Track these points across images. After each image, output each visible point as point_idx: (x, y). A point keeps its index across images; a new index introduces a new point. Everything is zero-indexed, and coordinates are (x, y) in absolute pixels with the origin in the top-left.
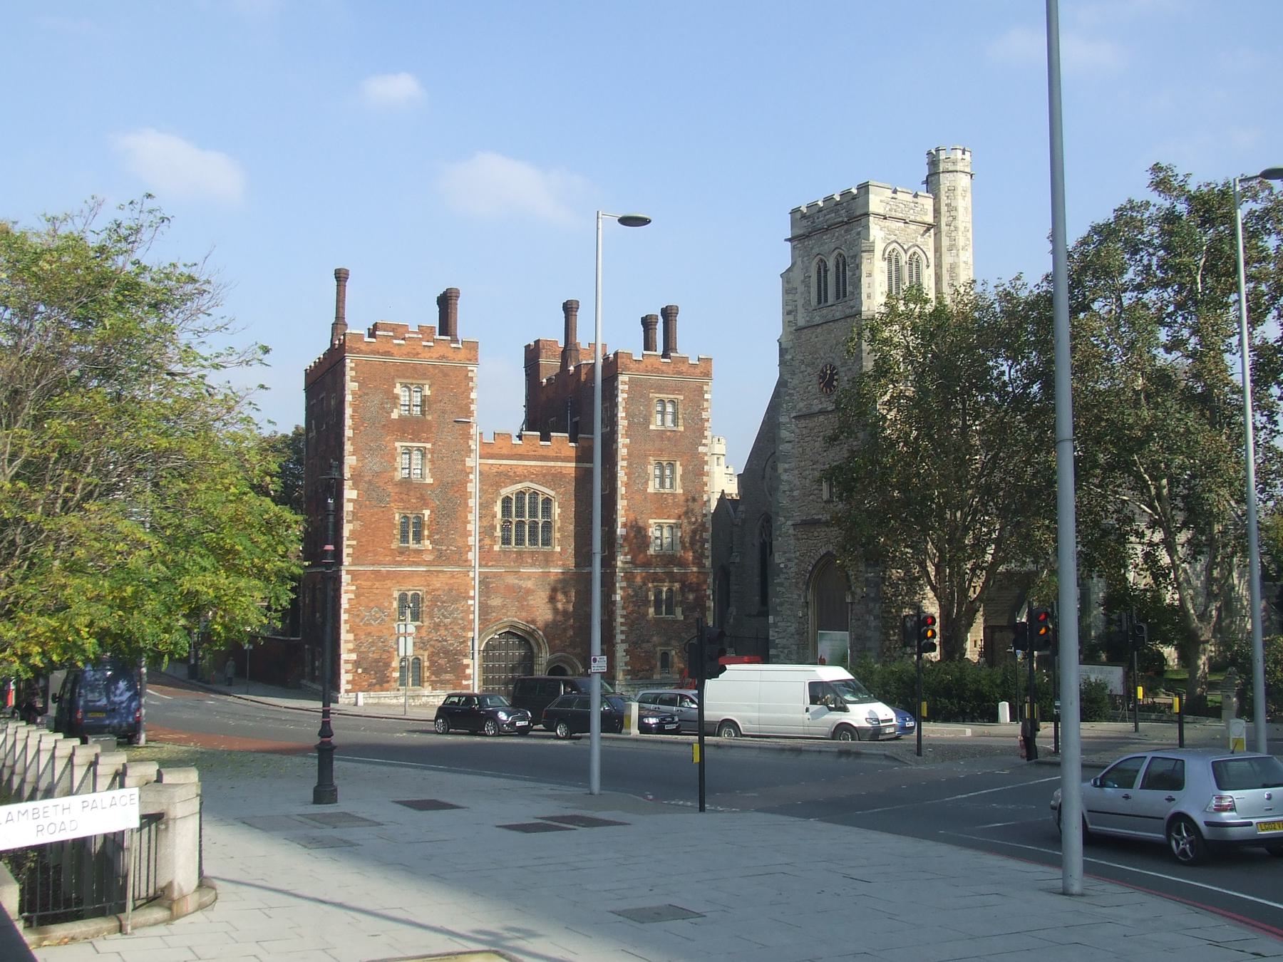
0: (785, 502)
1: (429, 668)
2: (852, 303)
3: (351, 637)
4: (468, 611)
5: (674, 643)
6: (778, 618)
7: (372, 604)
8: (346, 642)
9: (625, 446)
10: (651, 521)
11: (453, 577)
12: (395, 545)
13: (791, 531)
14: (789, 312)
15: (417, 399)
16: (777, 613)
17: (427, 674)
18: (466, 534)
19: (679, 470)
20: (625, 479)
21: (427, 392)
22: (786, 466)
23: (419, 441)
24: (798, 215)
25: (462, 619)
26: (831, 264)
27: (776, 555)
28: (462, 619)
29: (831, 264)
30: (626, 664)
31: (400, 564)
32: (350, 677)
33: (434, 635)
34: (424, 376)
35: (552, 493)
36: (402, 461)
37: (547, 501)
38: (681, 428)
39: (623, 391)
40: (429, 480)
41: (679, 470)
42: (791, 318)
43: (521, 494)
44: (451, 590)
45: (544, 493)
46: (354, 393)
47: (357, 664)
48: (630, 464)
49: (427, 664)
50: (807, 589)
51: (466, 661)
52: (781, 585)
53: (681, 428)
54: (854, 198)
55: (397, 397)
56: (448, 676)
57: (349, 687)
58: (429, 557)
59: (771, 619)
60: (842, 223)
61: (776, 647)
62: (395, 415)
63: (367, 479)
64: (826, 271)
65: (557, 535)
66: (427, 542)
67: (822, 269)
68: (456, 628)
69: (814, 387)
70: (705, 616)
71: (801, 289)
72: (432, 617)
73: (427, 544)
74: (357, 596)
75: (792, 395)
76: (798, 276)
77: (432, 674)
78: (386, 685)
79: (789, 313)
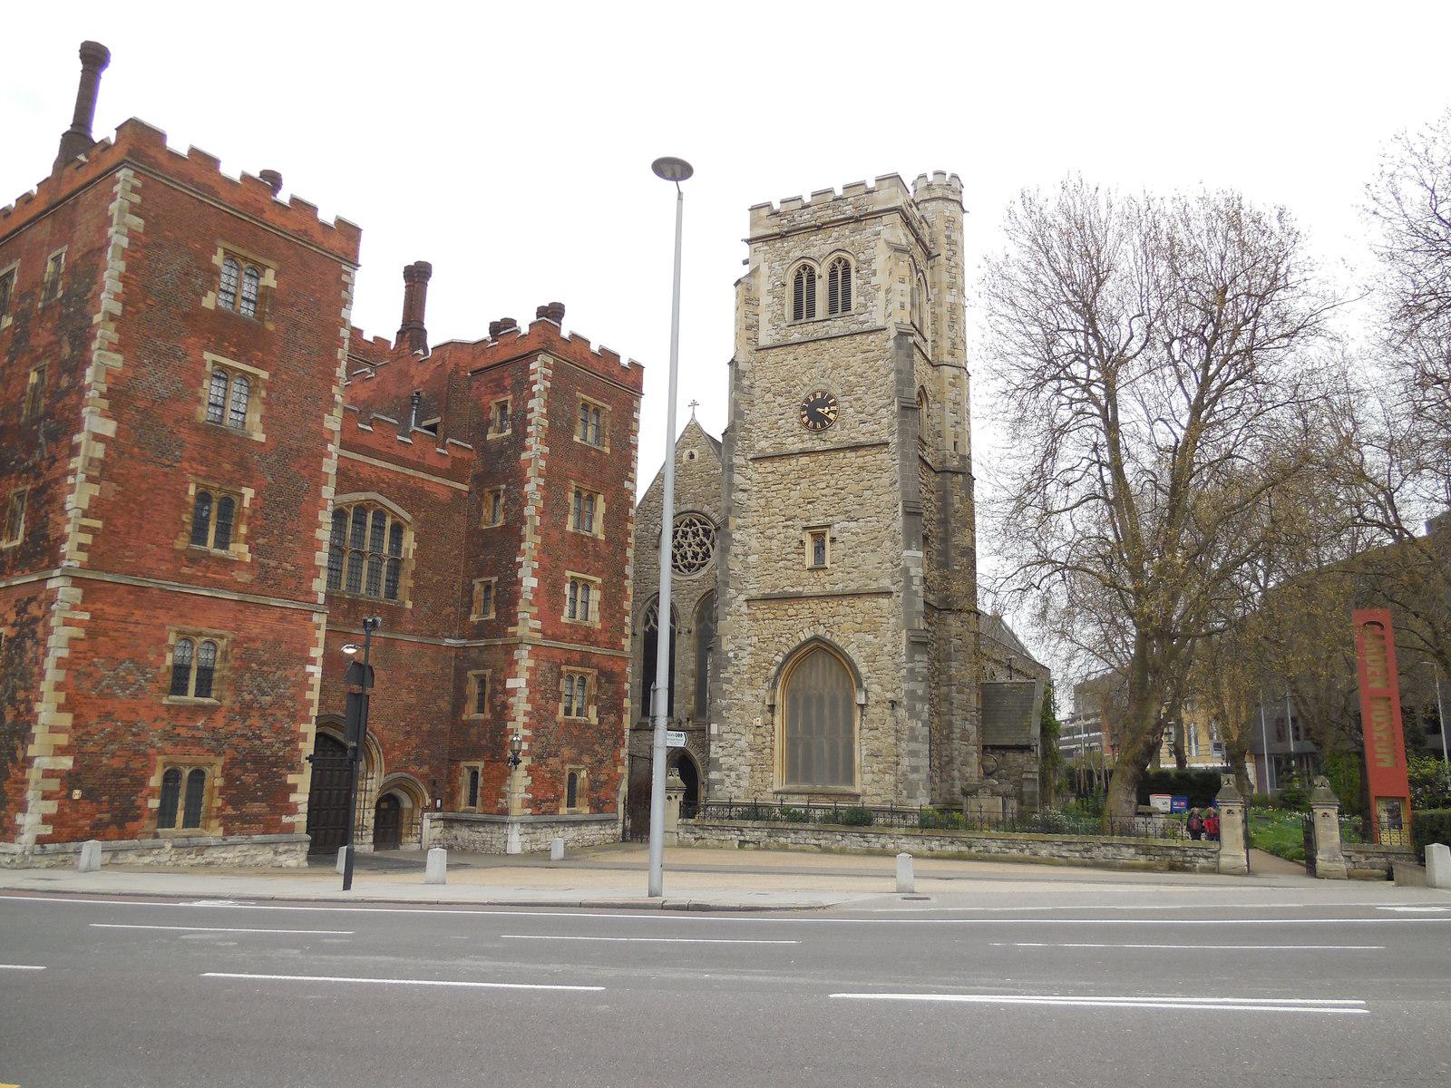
0: (736, 567)
1: (222, 791)
2: (861, 318)
3: (66, 719)
4: (304, 685)
5: (586, 759)
6: (724, 728)
7: (122, 654)
8: (54, 730)
9: (543, 456)
10: (568, 574)
11: (283, 619)
12: (182, 543)
13: (744, 609)
14: (748, 327)
15: (248, 289)
16: (722, 720)
17: (219, 803)
18: (314, 545)
19: (601, 506)
20: (541, 504)
21: (269, 279)
22: (739, 521)
23: (249, 363)
24: (765, 212)
25: (292, 698)
26: (822, 271)
27: (724, 640)
28: (292, 698)
29: (822, 271)
30: (527, 790)
31: (188, 580)
32: (51, 807)
33: (238, 726)
34: (269, 254)
35: (408, 517)
36: (212, 389)
37: (397, 530)
38: (607, 450)
39: (546, 377)
40: (260, 437)
41: (601, 506)
42: (751, 334)
43: (361, 510)
44: (277, 642)
45: (395, 514)
46: (132, 235)
47: (70, 779)
48: (548, 484)
49: (219, 782)
51: (291, 779)
52: (729, 681)
53: (607, 450)
54: (870, 192)
55: (216, 272)
56: (257, 808)
57: (48, 830)
58: (243, 577)
59: (714, 729)
60: (848, 220)
61: (719, 769)
62: (209, 302)
63: (141, 404)
64: (811, 280)
65: (406, 582)
66: (244, 548)
67: (805, 279)
68: (279, 714)
69: (793, 419)
70: (621, 719)
72: (238, 691)
73: (239, 550)
74: (92, 633)
75: (749, 431)
76: (763, 284)
77: (227, 802)
78: (130, 826)
79: (748, 328)
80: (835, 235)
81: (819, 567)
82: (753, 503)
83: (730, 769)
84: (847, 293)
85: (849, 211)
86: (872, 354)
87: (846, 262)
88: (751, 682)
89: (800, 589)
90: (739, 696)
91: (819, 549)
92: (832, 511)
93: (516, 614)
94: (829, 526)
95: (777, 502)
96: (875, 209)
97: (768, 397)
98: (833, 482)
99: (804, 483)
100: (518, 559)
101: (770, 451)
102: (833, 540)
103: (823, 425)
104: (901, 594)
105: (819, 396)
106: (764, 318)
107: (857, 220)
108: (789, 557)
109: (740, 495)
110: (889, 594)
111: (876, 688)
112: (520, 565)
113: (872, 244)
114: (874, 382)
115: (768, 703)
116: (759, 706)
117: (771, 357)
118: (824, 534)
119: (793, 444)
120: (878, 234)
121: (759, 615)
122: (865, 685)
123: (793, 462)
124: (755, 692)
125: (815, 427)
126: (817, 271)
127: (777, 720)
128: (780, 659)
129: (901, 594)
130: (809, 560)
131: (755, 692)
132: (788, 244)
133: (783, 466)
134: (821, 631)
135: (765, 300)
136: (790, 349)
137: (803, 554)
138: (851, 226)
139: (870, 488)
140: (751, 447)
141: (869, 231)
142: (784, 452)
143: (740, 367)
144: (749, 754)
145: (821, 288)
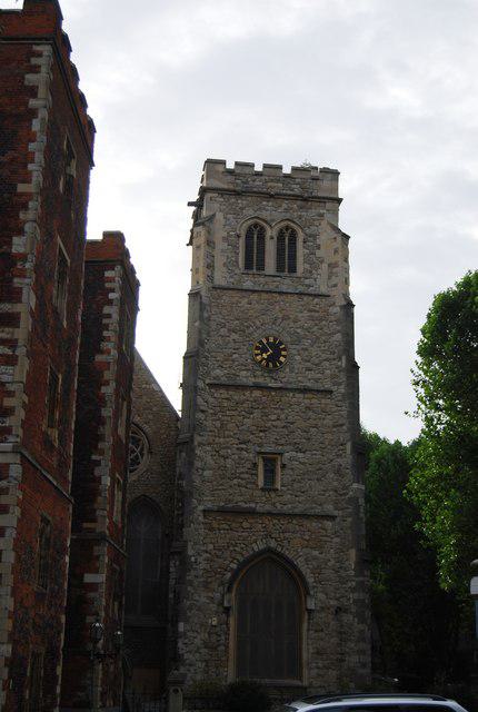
2: (307, 282)
16: (187, 621)
26: (271, 233)
50: (229, 590)
60: (296, 197)
64: (262, 237)
67: (255, 235)
71: (221, 245)
75: (206, 357)
80: (284, 206)
81: (269, 487)
82: (208, 423)
83: (191, 665)
84: (293, 257)
85: (297, 191)
86: (317, 314)
87: (293, 231)
88: (206, 585)
89: (253, 505)
90: (197, 598)
91: (270, 473)
92: (283, 441)
93: (95, 511)
94: (281, 454)
95: (230, 426)
96: (320, 195)
97: (223, 331)
98: (283, 416)
99: (257, 414)
100: (94, 457)
101: (224, 380)
102: (283, 466)
103: (275, 366)
104: (350, 519)
105: (271, 340)
106: (219, 261)
107: (305, 200)
108: (242, 476)
109: (200, 416)
110: (333, 518)
111: (321, 596)
112: (98, 463)
113: (316, 223)
114: (318, 338)
115: (226, 604)
116: (214, 607)
117: (226, 298)
118: (275, 460)
119: (245, 377)
120: (322, 215)
121: (215, 525)
122: (312, 593)
123: (247, 393)
124: (210, 594)
125: (267, 365)
126: (269, 233)
127: (232, 621)
128: (234, 566)
129: (350, 519)
130: (261, 483)
131: (210, 594)
132: (241, 202)
133: (237, 396)
134: (273, 544)
135: (221, 245)
136: (244, 294)
137: (257, 475)
138: (299, 203)
139: (316, 426)
140: (208, 373)
141: (313, 213)
142: (239, 383)
143: (205, 300)
144: (204, 651)
145: (271, 247)
